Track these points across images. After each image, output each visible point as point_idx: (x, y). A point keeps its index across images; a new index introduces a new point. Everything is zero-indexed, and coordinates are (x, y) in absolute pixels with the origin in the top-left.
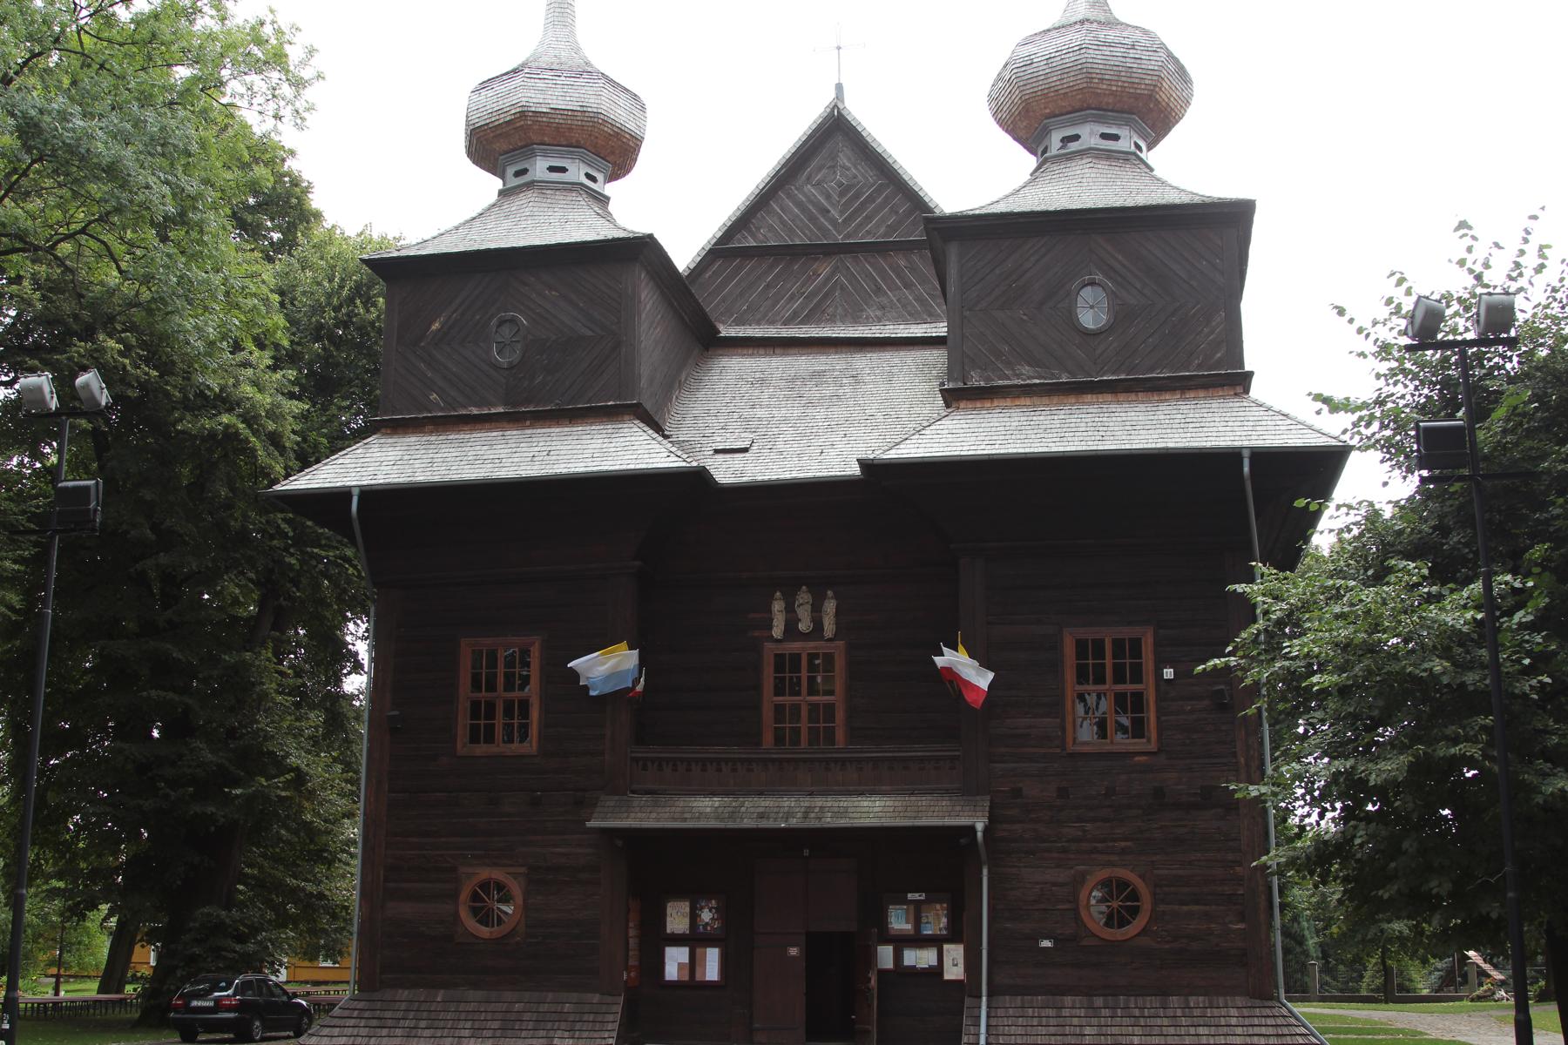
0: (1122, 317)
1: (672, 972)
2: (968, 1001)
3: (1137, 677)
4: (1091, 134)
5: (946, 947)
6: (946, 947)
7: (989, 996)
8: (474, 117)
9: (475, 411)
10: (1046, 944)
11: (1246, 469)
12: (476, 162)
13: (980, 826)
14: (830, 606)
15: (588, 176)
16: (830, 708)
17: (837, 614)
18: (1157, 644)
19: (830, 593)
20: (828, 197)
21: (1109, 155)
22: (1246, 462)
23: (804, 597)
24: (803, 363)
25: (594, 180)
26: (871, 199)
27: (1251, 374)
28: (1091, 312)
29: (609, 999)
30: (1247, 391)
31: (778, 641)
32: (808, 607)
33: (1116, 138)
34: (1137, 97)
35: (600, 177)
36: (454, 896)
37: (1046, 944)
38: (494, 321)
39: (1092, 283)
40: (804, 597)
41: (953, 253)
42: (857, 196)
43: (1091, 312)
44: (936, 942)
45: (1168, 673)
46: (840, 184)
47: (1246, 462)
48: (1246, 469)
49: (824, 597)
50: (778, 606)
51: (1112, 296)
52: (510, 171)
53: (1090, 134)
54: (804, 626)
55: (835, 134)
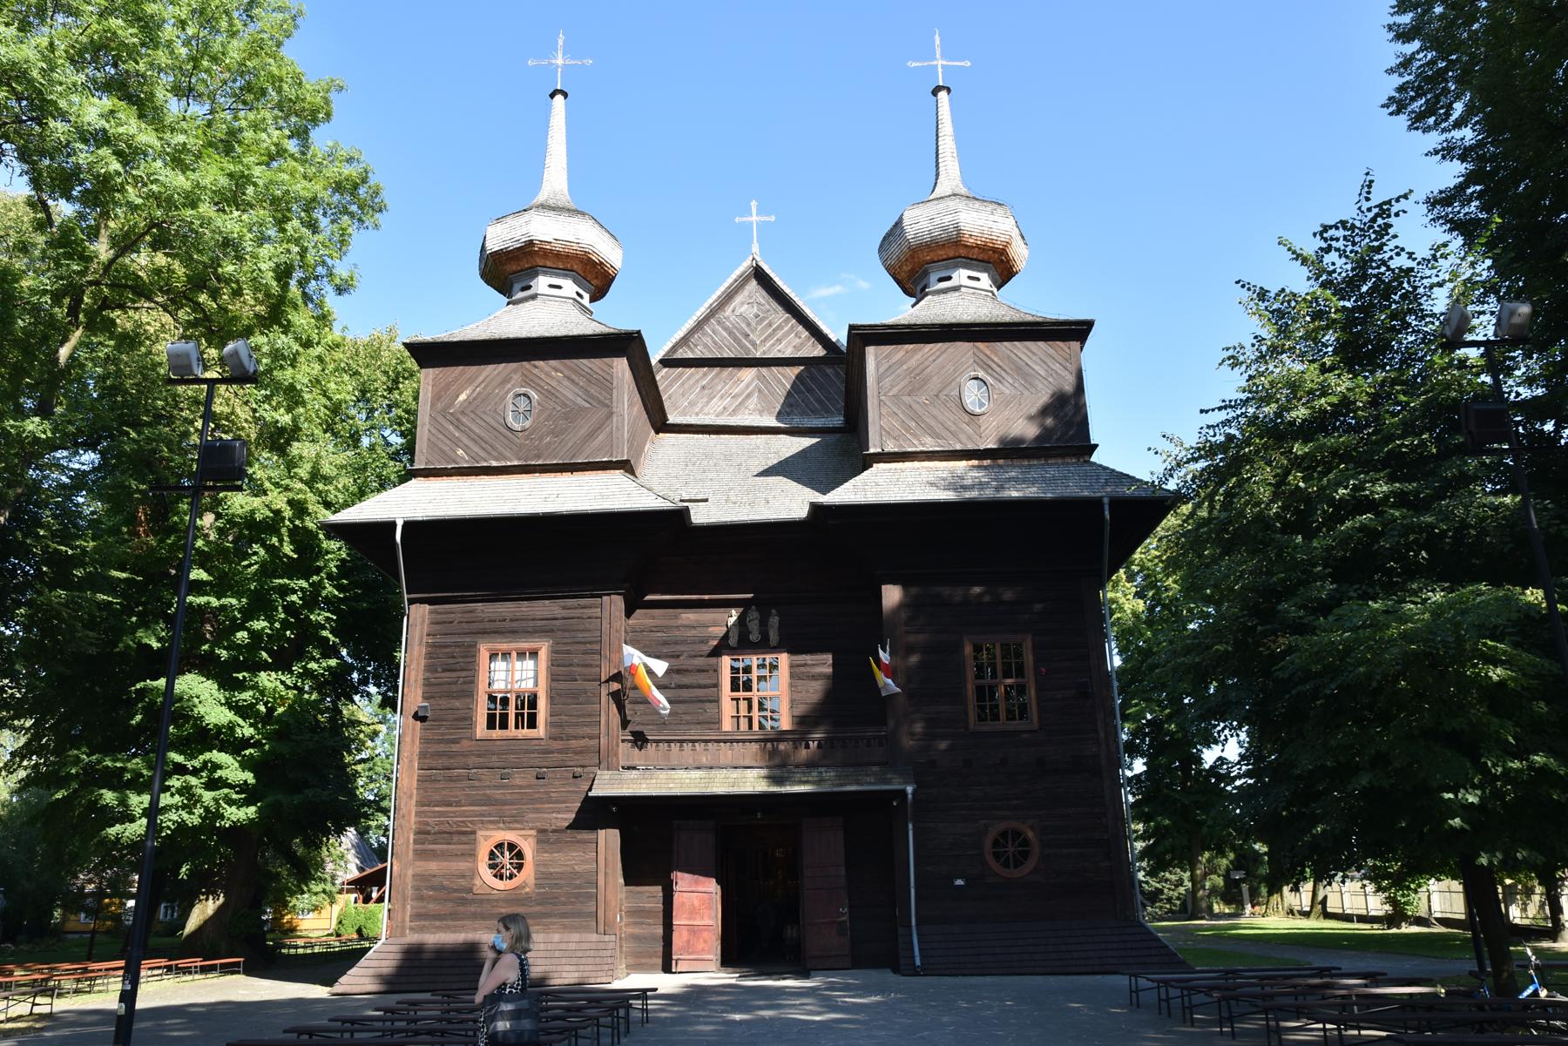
2: (901, 931)
9: (494, 464)
10: (959, 882)
12: (488, 282)
14: (774, 621)
18: (1035, 648)
20: (749, 324)
22: (1107, 507)
26: (779, 327)
34: (994, 250)
35: (587, 296)
36: (472, 855)
37: (959, 882)
38: (511, 395)
41: (871, 353)
47: (1107, 507)
49: (770, 614)
52: (517, 286)
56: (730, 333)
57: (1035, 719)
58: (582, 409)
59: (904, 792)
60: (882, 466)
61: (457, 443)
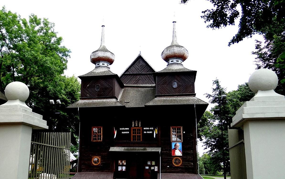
0: (179, 86)
1: (119, 170)
3: (180, 133)
4: (175, 61)
5: (155, 167)
6: (155, 167)
7: (161, 173)
8: (93, 57)
10: (168, 166)
11: (195, 107)
13: (160, 152)
14: (140, 123)
15: (107, 65)
16: (140, 136)
17: (141, 124)
20: (139, 67)
21: (177, 64)
23: (136, 122)
24: (136, 89)
25: (108, 65)
26: (145, 67)
28: (175, 85)
29: (112, 173)
30: (195, 96)
35: (109, 65)
37: (168, 166)
38: (96, 85)
39: (175, 82)
40: (136, 122)
42: (143, 67)
44: (154, 166)
45: (184, 132)
46: (140, 65)
47: (195, 106)
48: (195, 107)
51: (177, 83)
53: (175, 61)
55: (140, 58)
56: (135, 69)
58: (108, 88)
61: (87, 93)
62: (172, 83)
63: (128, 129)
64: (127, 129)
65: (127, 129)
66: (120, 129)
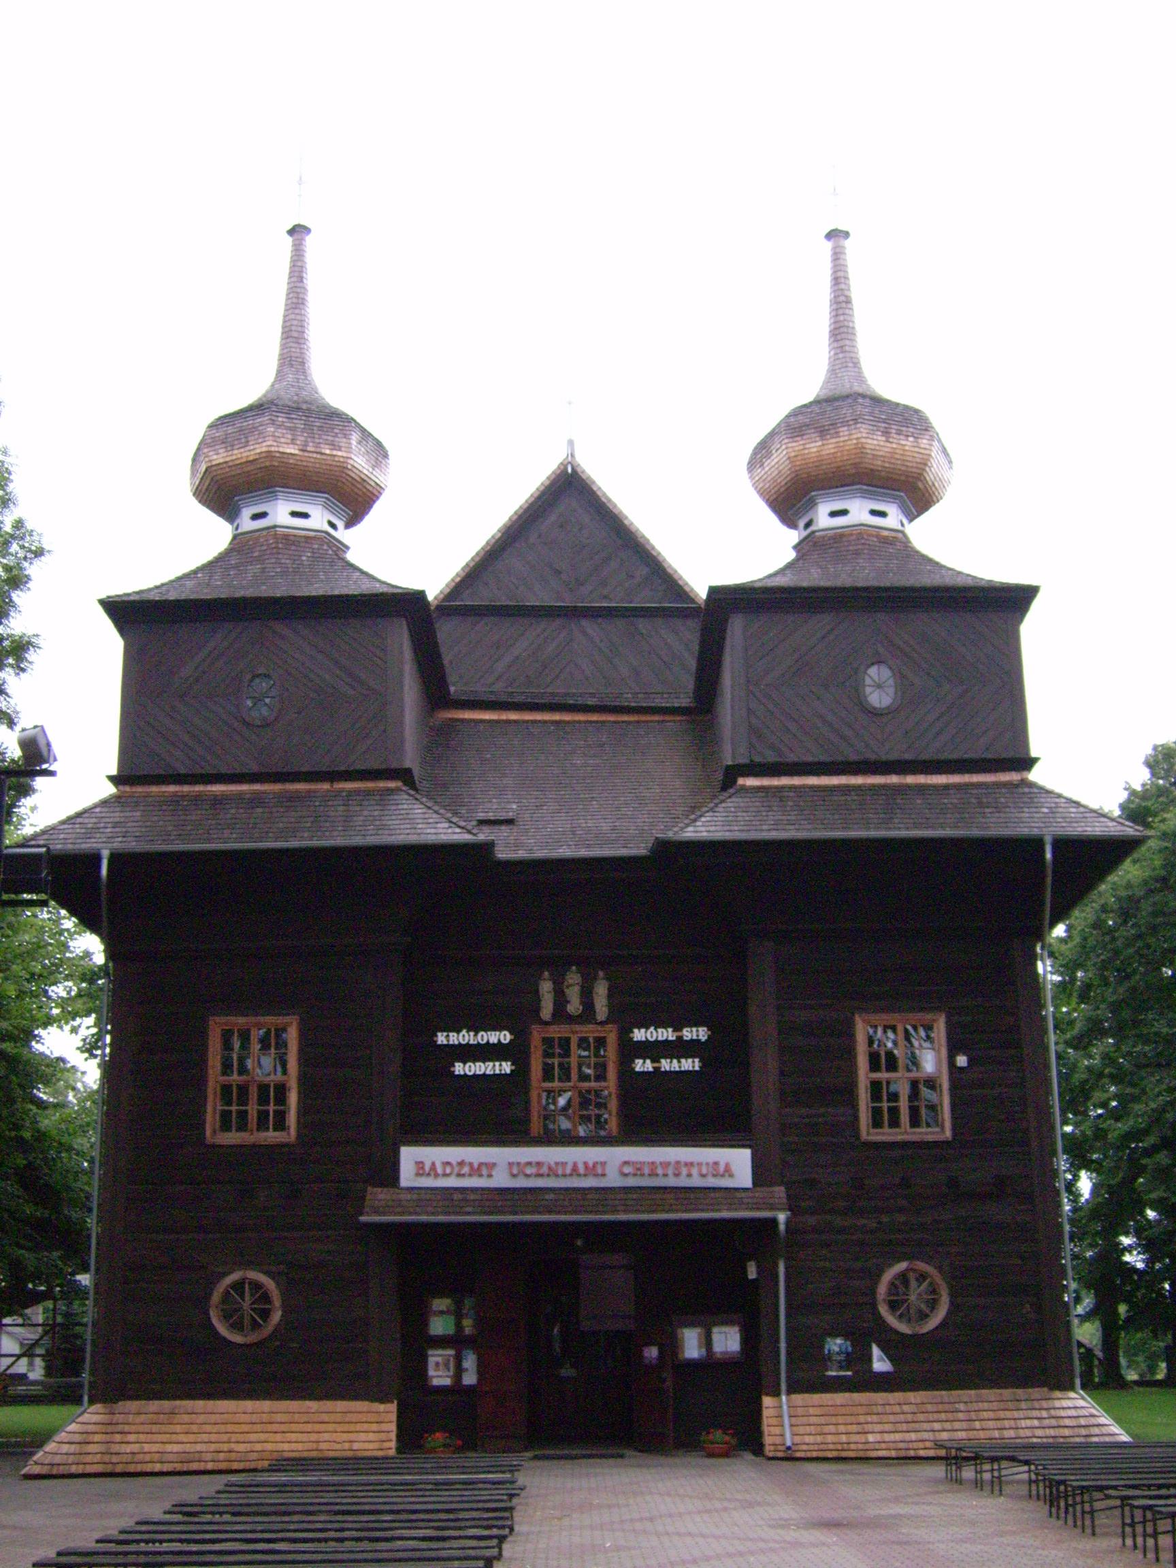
11: (1048, 856)
14: (601, 990)
17: (610, 996)
19: (601, 974)
23: (573, 978)
27: (1035, 760)
31: (547, 1023)
32: (577, 989)
33: (882, 514)
35: (340, 524)
40: (573, 978)
41: (737, 628)
43: (879, 688)
48: (1048, 856)
50: (546, 987)
51: (900, 676)
52: (247, 513)
54: (574, 1006)
55: (568, 491)
57: (948, 1124)
59: (774, 1222)
60: (751, 782)
62: (856, 671)
63: (505, 1037)
64: (493, 1037)
65: (493, 1037)
66: (441, 1038)
